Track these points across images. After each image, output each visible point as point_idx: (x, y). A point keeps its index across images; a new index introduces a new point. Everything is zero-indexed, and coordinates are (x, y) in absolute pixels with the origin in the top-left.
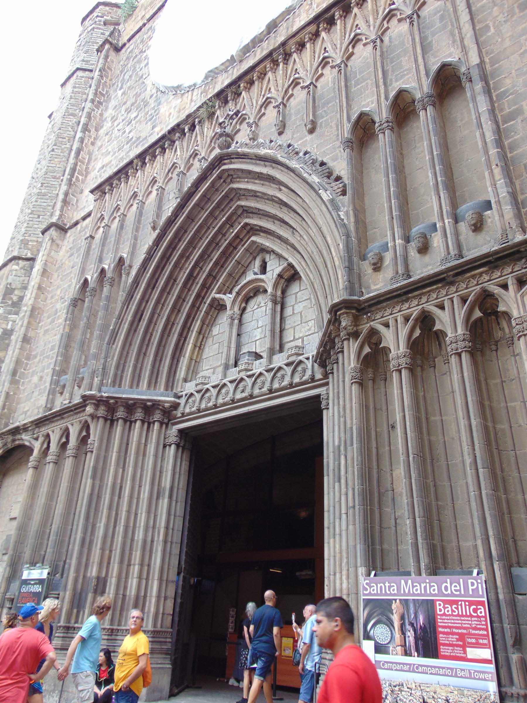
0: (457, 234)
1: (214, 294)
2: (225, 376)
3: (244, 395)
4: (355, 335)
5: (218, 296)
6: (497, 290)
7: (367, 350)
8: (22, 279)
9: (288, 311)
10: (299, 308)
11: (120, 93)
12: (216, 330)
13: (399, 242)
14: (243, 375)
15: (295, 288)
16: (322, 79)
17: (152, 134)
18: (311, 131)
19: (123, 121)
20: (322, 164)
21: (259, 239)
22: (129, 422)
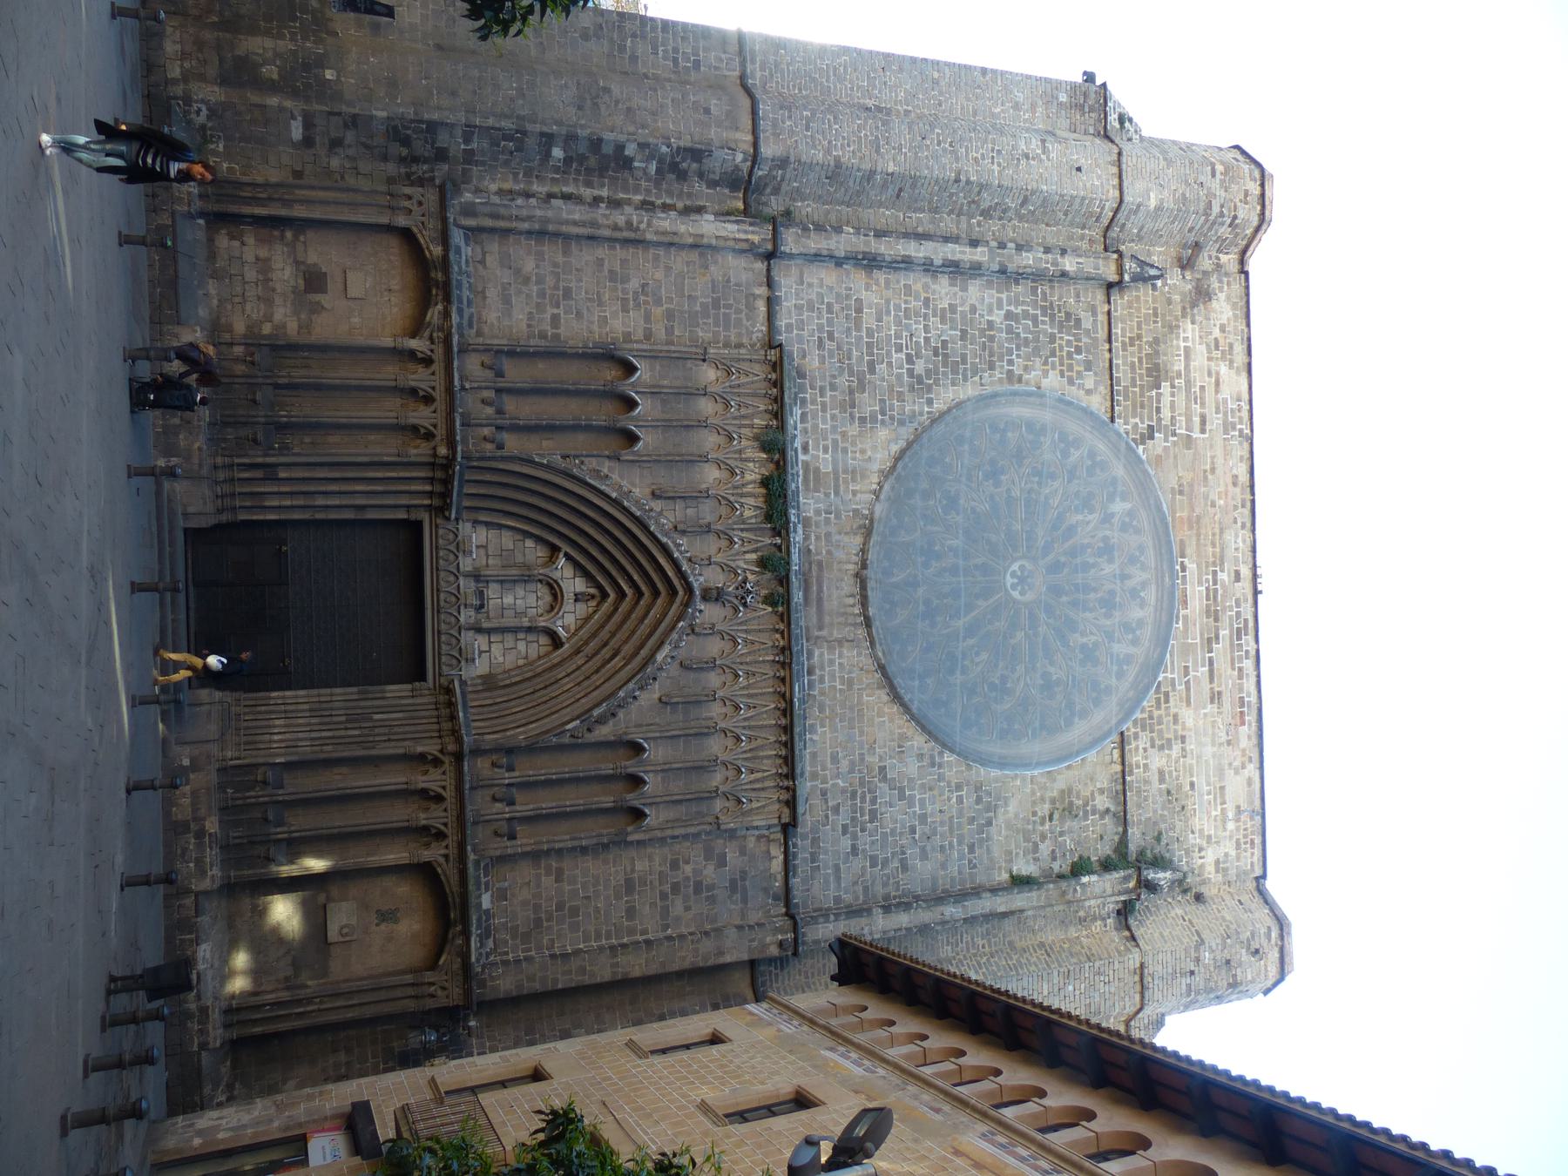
0: (497, 820)
1: (566, 548)
2: (467, 575)
3: (442, 603)
4: (441, 751)
5: (561, 555)
6: (444, 844)
7: (430, 757)
8: (718, 170)
9: (521, 636)
10: (521, 646)
11: (997, 317)
12: (529, 543)
13: (507, 781)
14: (462, 601)
15: (544, 640)
16: (721, 704)
17: (852, 417)
18: (660, 699)
19: (927, 340)
20: (614, 715)
21: (607, 606)
22: (431, 480)
